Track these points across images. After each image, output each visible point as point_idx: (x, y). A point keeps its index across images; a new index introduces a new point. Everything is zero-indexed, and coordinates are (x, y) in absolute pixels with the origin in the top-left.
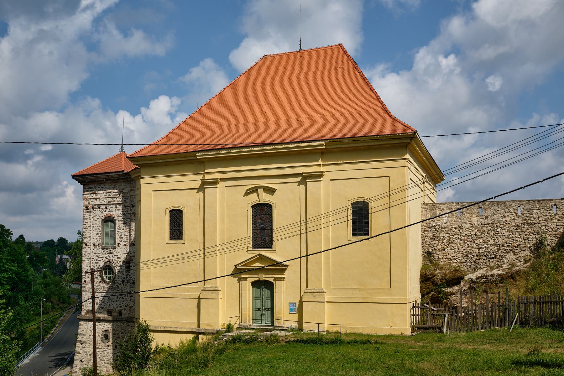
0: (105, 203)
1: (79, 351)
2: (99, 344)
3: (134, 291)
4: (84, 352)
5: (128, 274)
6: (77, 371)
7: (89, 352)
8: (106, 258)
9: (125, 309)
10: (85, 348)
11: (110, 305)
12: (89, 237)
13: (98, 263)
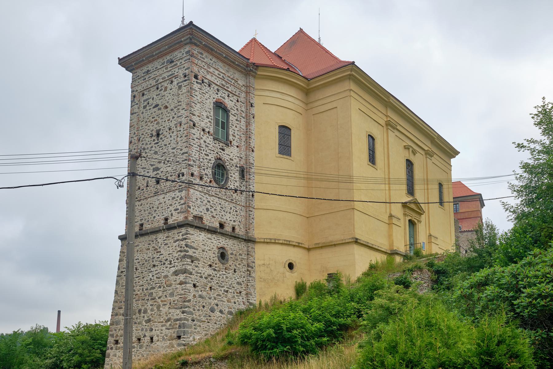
0: (218, 84)
1: (191, 270)
2: (216, 264)
3: (254, 206)
4: (198, 273)
5: (242, 183)
6: (191, 300)
7: (204, 274)
9: (238, 225)
10: (199, 267)
11: (222, 216)
12: (199, 116)
13: (208, 155)
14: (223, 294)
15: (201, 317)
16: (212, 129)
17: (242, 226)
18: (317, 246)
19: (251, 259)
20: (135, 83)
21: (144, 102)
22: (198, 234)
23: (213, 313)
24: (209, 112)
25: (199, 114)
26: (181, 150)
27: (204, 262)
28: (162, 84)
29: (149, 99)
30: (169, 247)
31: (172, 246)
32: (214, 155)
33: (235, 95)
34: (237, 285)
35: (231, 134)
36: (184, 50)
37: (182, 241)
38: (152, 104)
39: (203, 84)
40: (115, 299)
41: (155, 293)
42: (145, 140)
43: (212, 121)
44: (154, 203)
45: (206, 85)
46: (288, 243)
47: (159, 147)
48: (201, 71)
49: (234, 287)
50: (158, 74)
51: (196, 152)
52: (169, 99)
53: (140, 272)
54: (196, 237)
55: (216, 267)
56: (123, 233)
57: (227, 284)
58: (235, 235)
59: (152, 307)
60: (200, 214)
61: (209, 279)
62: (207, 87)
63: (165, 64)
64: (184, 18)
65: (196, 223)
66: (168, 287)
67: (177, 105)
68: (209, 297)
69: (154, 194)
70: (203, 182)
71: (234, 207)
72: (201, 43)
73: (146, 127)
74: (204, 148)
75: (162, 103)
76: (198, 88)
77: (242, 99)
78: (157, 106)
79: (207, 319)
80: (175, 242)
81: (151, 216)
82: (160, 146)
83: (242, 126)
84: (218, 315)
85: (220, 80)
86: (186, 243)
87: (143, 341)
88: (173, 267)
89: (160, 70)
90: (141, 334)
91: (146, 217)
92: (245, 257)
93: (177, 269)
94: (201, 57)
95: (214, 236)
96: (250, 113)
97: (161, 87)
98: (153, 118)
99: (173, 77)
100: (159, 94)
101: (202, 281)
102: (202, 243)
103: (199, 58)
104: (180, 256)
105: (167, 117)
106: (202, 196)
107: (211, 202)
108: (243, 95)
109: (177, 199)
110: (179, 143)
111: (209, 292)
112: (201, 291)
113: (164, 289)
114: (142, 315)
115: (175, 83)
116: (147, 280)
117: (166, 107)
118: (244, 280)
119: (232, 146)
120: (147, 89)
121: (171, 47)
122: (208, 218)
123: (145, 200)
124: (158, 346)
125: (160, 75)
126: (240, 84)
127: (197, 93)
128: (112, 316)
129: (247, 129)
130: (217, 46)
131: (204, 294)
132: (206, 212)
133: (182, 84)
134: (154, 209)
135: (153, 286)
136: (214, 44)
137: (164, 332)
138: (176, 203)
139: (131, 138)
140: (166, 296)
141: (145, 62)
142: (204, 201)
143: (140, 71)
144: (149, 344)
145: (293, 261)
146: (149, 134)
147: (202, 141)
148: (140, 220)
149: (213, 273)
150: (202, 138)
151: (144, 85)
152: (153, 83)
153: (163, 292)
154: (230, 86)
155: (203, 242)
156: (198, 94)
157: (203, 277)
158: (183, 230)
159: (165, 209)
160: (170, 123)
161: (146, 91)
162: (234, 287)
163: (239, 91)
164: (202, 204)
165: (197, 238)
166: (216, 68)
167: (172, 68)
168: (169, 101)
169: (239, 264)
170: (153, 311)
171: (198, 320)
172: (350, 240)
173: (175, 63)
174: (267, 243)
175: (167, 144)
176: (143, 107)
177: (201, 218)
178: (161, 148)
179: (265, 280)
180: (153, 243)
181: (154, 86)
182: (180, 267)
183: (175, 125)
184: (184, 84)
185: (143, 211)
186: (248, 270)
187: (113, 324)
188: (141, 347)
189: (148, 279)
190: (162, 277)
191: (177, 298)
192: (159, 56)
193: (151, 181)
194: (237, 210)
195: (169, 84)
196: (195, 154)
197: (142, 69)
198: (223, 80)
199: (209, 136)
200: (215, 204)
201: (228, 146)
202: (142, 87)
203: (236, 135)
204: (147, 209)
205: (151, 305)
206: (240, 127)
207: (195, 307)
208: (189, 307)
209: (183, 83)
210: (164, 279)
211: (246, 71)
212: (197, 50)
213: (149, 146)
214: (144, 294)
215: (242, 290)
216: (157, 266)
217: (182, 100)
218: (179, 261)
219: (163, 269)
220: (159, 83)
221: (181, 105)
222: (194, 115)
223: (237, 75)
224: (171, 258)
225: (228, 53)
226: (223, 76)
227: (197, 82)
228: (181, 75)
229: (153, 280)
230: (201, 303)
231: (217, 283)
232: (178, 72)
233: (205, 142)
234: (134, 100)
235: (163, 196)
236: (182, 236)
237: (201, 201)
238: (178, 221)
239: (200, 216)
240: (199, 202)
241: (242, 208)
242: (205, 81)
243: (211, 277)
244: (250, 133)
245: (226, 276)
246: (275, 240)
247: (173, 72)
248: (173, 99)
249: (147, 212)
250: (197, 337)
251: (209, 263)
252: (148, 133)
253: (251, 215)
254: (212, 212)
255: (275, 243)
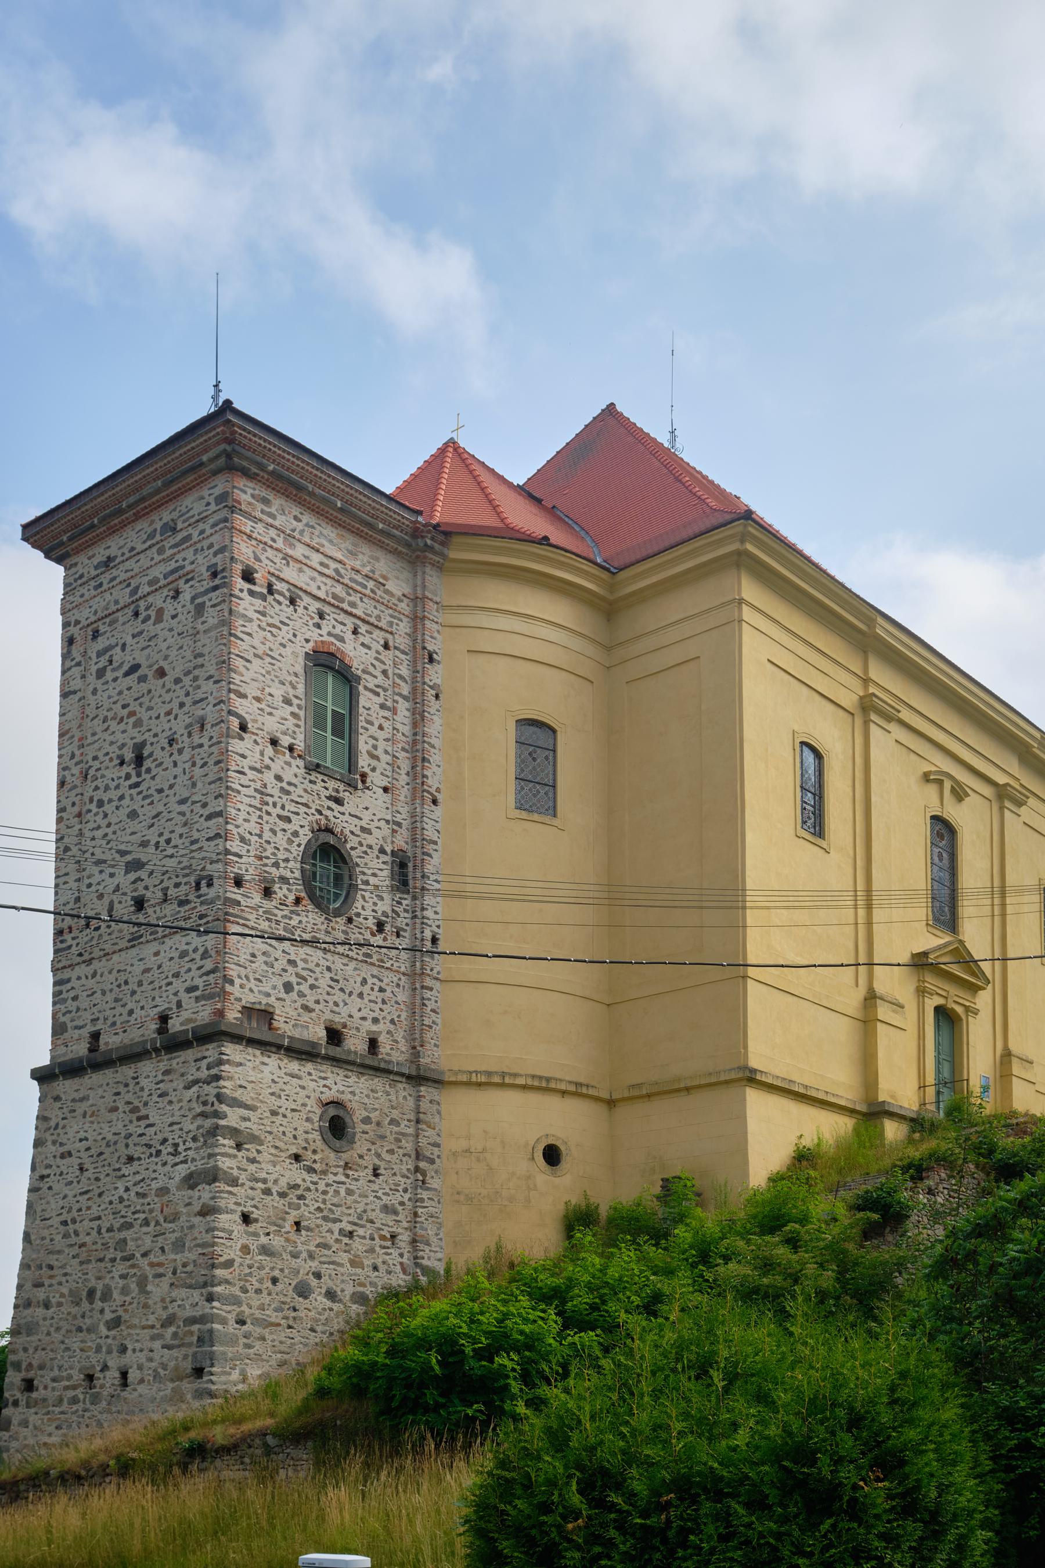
0: (321, 594)
1: (235, 1172)
2: (315, 1152)
4: (257, 1180)
7: (276, 1181)
8: (320, 812)
10: (259, 1162)
11: (336, 1004)
12: (258, 699)
13: (288, 820)
14: (337, 1241)
15: (267, 1312)
16: (301, 737)
17: (400, 1036)
18: (636, 1092)
19: (426, 1134)
20: (71, 598)
21: (98, 656)
22: (257, 1063)
23: (306, 1298)
24: (291, 683)
25: (258, 694)
26: (205, 805)
27: (276, 1147)
28: (150, 599)
29: (110, 648)
30: (170, 1102)
31: (180, 1101)
32: (309, 818)
33: (377, 627)
34: (382, 1215)
35: (364, 751)
36: (211, 491)
37: (208, 1084)
38: (122, 663)
39: (270, 598)
40: (23, 1258)
41: (132, 1240)
42: (103, 776)
43: (302, 713)
44: (129, 969)
45: (280, 598)
46: (544, 1084)
47: (141, 796)
48: (263, 558)
49: (372, 1222)
50: (136, 570)
51: (251, 810)
52: (168, 648)
53: (93, 1177)
54: (251, 1073)
55: (315, 1161)
56: (44, 1059)
57: (352, 1211)
58: (376, 1064)
59: (125, 1282)
60: (264, 1002)
61: (292, 1197)
62: (283, 607)
63: (158, 537)
64: (221, 387)
65: (254, 1029)
66: (170, 1222)
67: (192, 665)
68: (291, 1252)
69: (129, 941)
70: (274, 903)
71: (373, 976)
72: (262, 467)
73: (106, 736)
74: (276, 799)
75: (151, 661)
76: (256, 611)
77: (401, 640)
78: (135, 668)
79: (286, 1318)
80: (187, 1087)
81: (122, 1010)
82: (145, 793)
83: (399, 726)
84: (321, 1306)
85: (329, 581)
86: (218, 1090)
87: (101, 1381)
88: (182, 1162)
89: (142, 556)
90: (94, 1361)
91: (108, 1013)
92: (411, 1131)
93: (193, 1168)
94: (262, 512)
95: (309, 1066)
96: (424, 683)
97: (147, 609)
98: (124, 707)
99: (180, 577)
100: (141, 633)
101: (271, 1203)
102: (271, 1091)
103: (258, 514)
104: (201, 1131)
105: (164, 703)
106: (270, 945)
107: (301, 964)
108: (404, 627)
109: (194, 956)
110: (199, 785)
111: (293, 1236)
112: (268, 1234)
113: (158, 1228)
114: (98, 1304)
115: (186, 596)
116: (111, 1203)
117: (161, 673)
118: (406, 1200)
119: (368, 788)
120: (106, 616)
121: (172, 481)
122: (291, 1013)
123: (104, 959)
124: (141, 1396)
125: (144, 571)
126: (395, 591)
127: (252, 628)
128: (16, 1307)
129: (415, 734)
130: (316, 475)
131: (277, 1242)
132: (283, 995)
133: (205, 598)
134: (130, 986)
135: (128, 1220)
136: (303, 468)
137: (156, 1356)
138: (189, 970)
139: (65, 769)
140: (162, 1249)
141: (98, 532)
142: (277, 960)
143: (86, 561)
144: (115, 1390)
145: (558, 1138)
146: (114, 756)
147: (269, 777)
148: (92, 1020)
149: (304, 1180)
150: (268, 768)
151: (98, 603)
152: (123, 596)
153: (155, 1236)
154: (361, 599)
155: (273, 1085)
156: (256, 628)
157: (274, 1191)
158: (210, 1051)
159: (160, 987)
160: (173, 721)
161: (104, 623)
162: (372, 1222)
163: (391, 616)
164: (270, 970)
165: (253, 1076)
166: (313, 544)
167: (176, 550)
168: (168, 652)
169: (391, 1152)
170: (127, 1295)
171: (256, 1322)
172: (733, 1075)
173: (184, 534)
174: (479, 1084)
175: (166, 787)
176: (94, 674)
177: (267, 1015)
178: (148, 801)
179: (469, 1199)
180: (128, 1092)
181: (125, 606)
182: (203, 1162)
183: (186, 728)
184: (210, 600)
185: (98, 995)
186: (417, 1169)
187: (19, 1333)
188: (95, 1399)
189: (113, 1199)
190: (153, 1192)
191: (191, 1256)
192: (138, 512)
193: (120, 902)
194: (383, 985)
195: (169, 600)
196: (247, 817)
197: (90, 554)
198: (338, 581)
199: (292, 761)
200: (311, 971)
201: (356, 788)
202: (93, 610)
203: (379, 752)
204: (110, 987)
205: (123, 1277)
206: (394, 729)
207: (247, 1281)
208: (227, 1282)
209: (210, 595)
210: (156, 1199)
211: (414, 551)
212: (250, 491)
213: (114, 794)
214: (103, 1244)
215: (400, 1230)
216: (139, 1159)
217: (206, 650)
218: (199, 1144)
219: (155, 1168)
220: (141, 598)
221: (202, 666)
222: (244, 696)
223: (384, 565)
224: (176, 1137)
225: (352, 495)
226: (336, 571)
227: (251, 593)
228: (204, 569)
229: (126, 1203)
230: (267, 1270)
231: (319, 1209)
232: (192, 563)
233: (278, 778)
234: (69, 652)
235: (153, 947)
236: (208, 1069)
237: (266, 963)
238: (198, 1023)
239: (263, 1008)
240: (259, 964)
241: (400, 979)
242: (278, 586)
243: (299, 1192)
244: (426, 745)
245: (347, 1189)
246: (503, 1075)
247: (181, 563)
248: (181, 648)
249: (110, 997)
250: (254, 1372)
251: (294, 1150)
252: (111, 755)
253: (429, 999)
254: (301, 994)
255: (502, 1085)
